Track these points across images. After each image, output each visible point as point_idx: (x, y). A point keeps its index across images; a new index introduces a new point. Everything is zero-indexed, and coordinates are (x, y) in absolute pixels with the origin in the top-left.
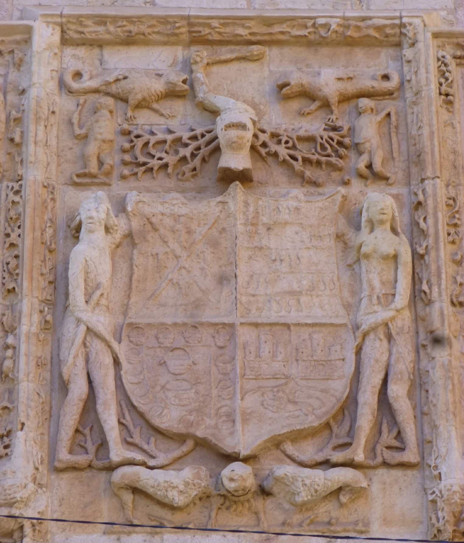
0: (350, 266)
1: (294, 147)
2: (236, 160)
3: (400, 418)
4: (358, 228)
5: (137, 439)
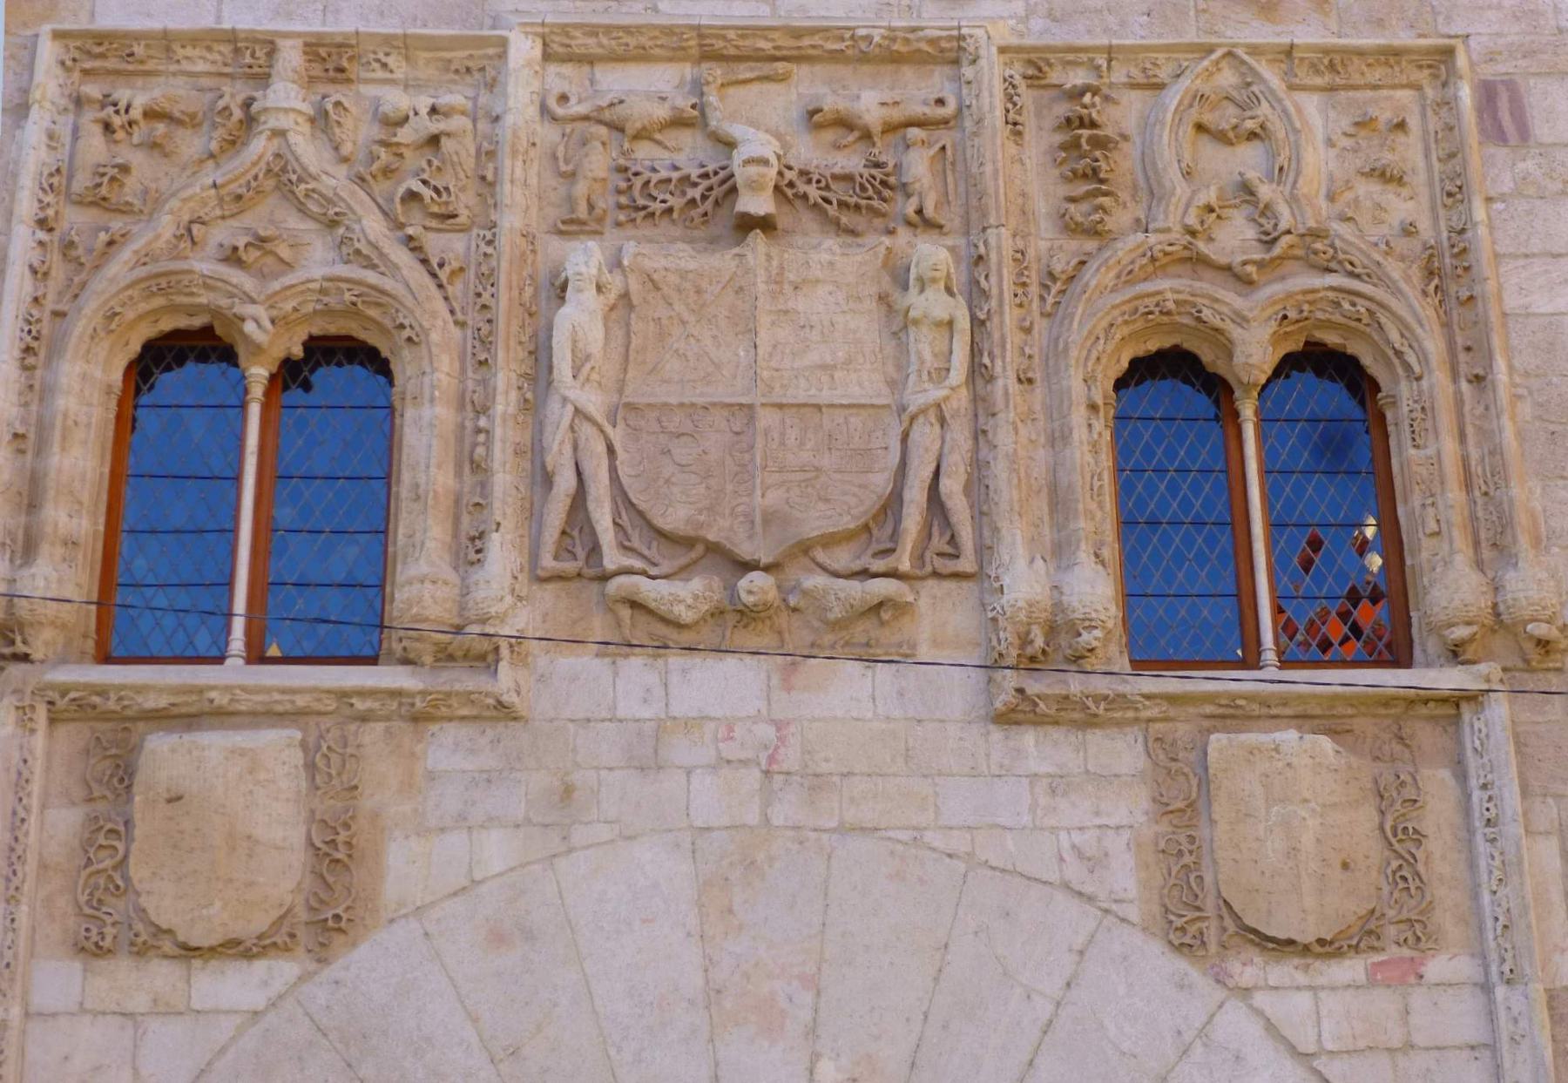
0: (894, 333)
1: (827, 188)
2: (757, 203)
3: (954, 520)
4: (906, 288)
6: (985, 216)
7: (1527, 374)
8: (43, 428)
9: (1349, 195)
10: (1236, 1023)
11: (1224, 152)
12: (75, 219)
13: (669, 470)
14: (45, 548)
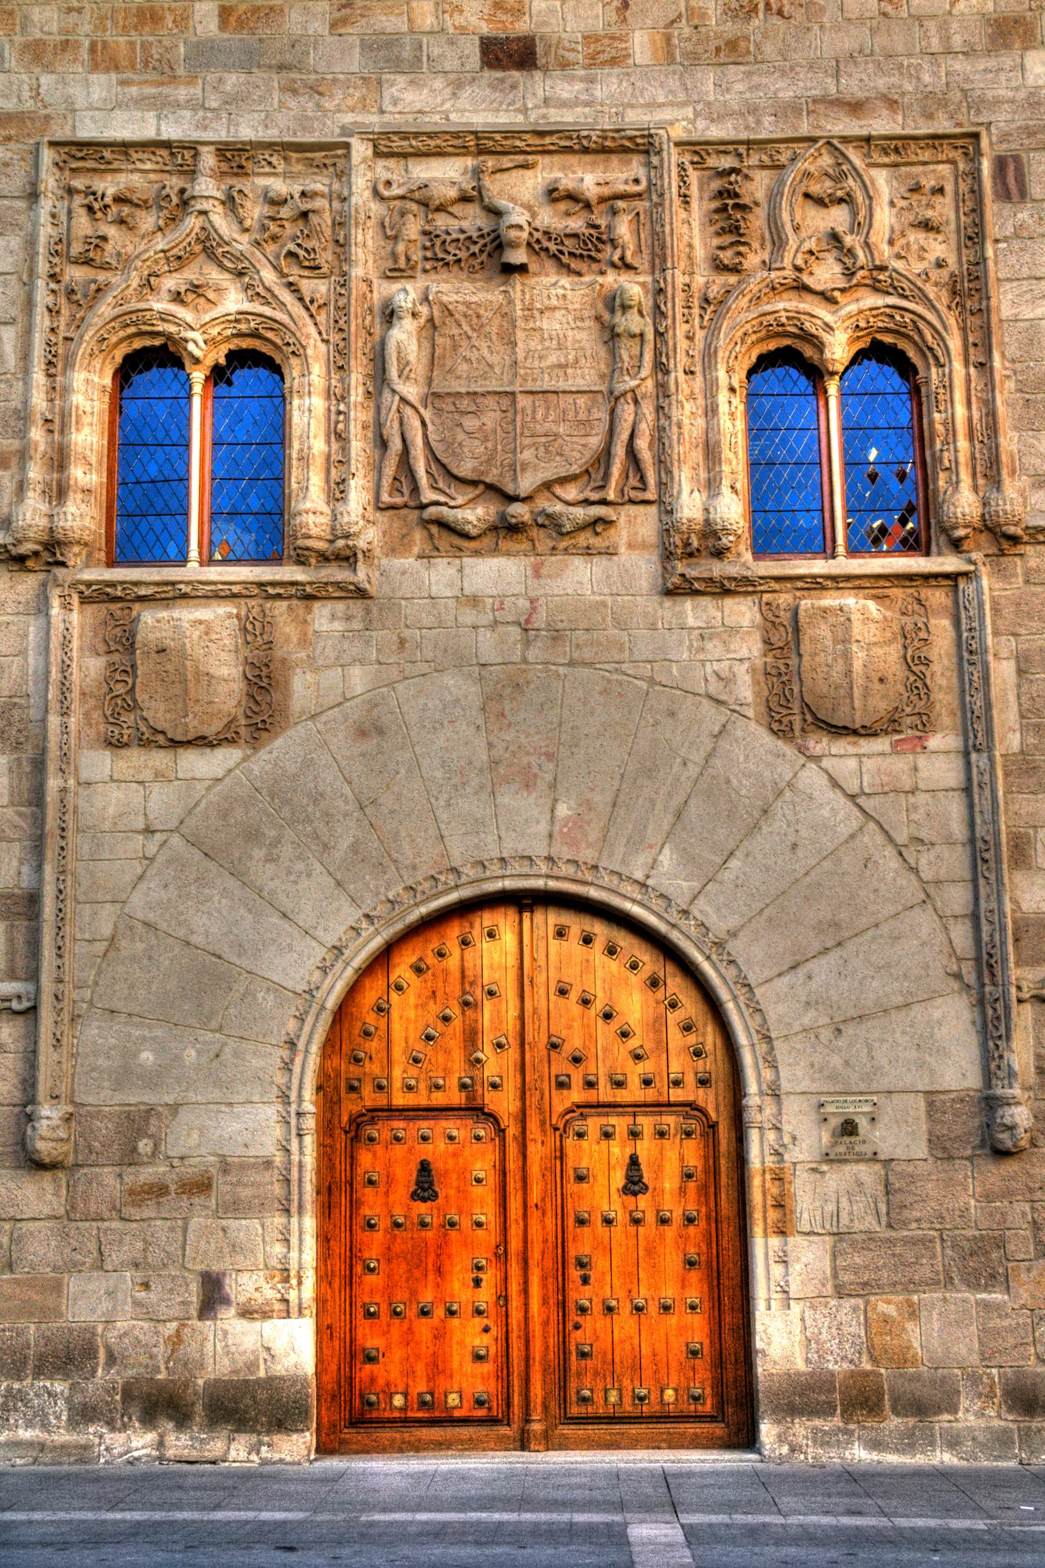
5: (441, 485)
6: (665, 261)
7: (1013, 361)
9: (903, 241)
10: (812, 777)
11: (823, 212)
12: (76, 274)
13: (461, 436)
14: (71, 494)
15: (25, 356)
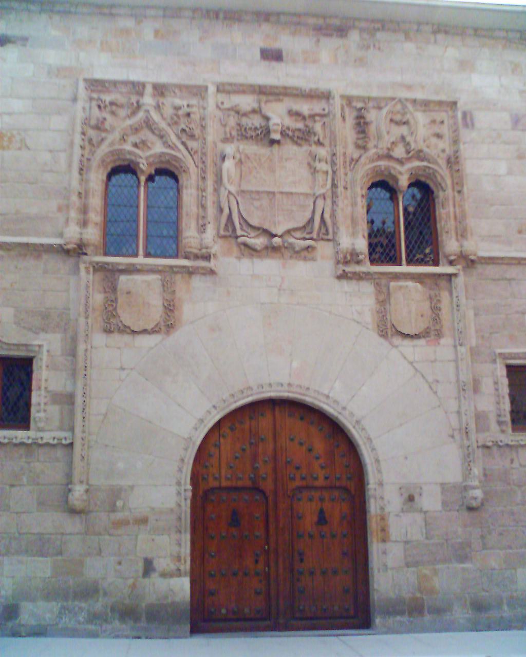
2: (277, 136)
8: (87, 192)
12: (92, 133)
15: (70, 166)
